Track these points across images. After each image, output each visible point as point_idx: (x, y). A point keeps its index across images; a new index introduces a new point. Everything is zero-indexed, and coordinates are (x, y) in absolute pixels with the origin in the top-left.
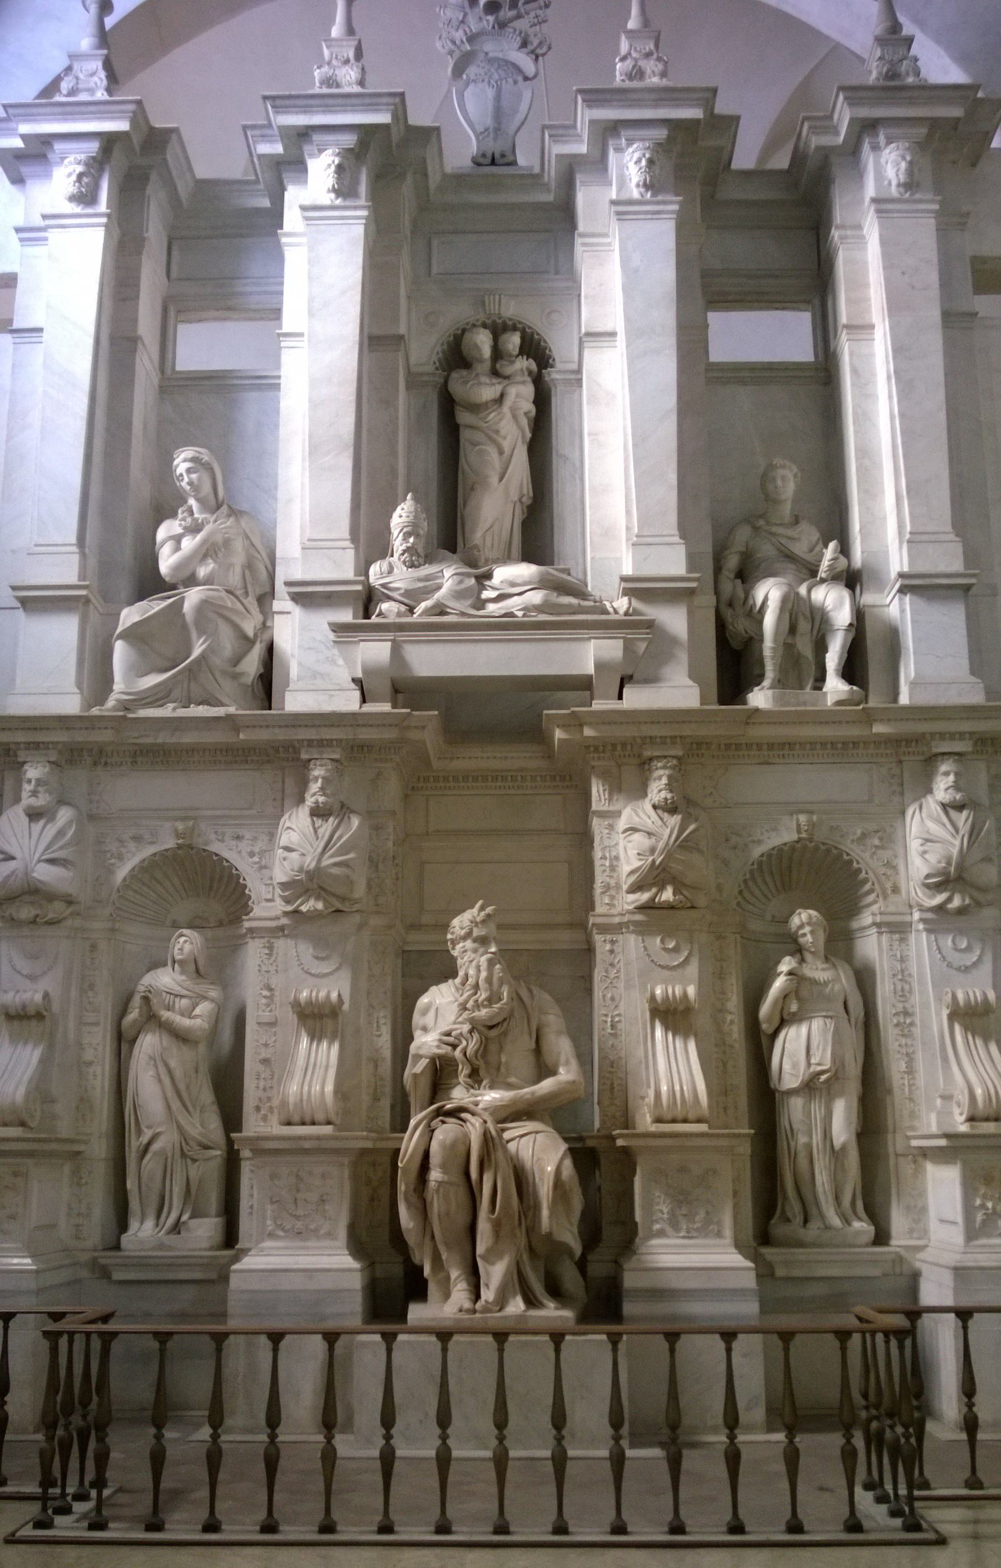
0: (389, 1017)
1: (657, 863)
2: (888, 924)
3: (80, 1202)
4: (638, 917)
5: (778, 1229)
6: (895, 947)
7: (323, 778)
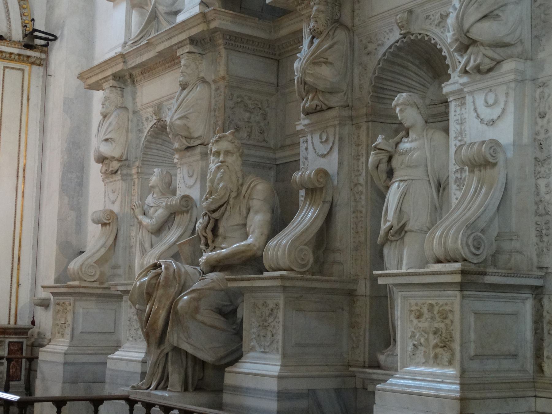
6: (458, 112)
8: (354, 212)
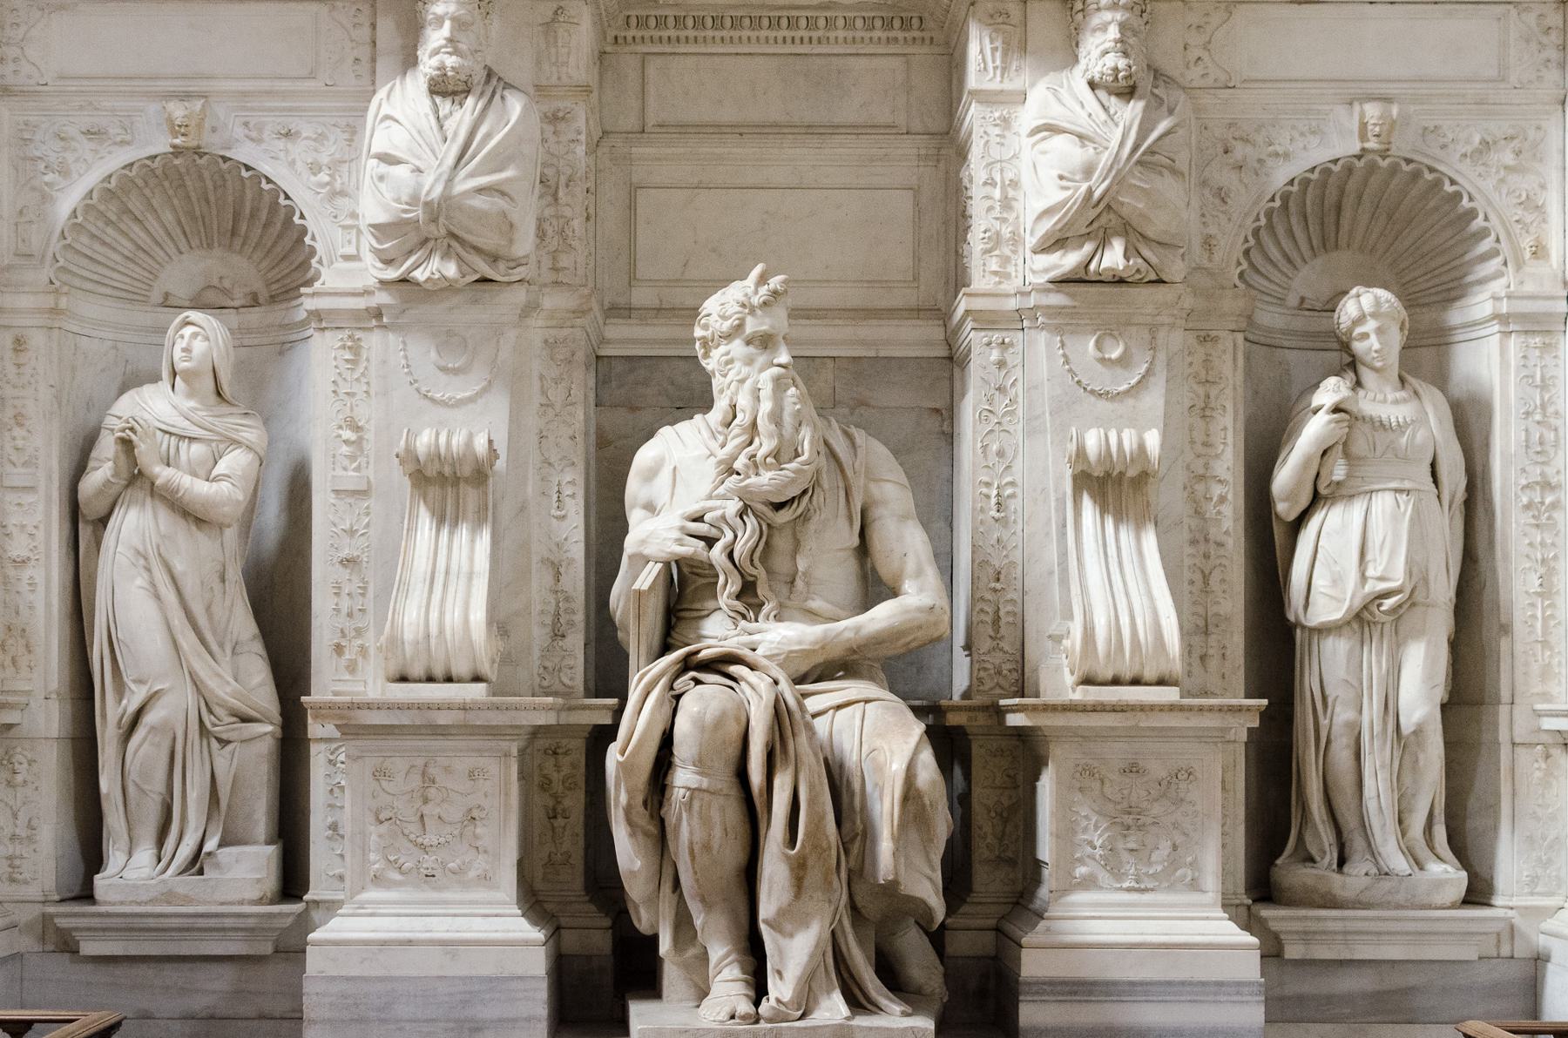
0: (581, 482)
1: (1097, 194)
2: (1523, 317)
3: (15, 816)
4: (1057, 299)
5: (1291, 873)
7: (454, 19)
8: (1194, 542)
